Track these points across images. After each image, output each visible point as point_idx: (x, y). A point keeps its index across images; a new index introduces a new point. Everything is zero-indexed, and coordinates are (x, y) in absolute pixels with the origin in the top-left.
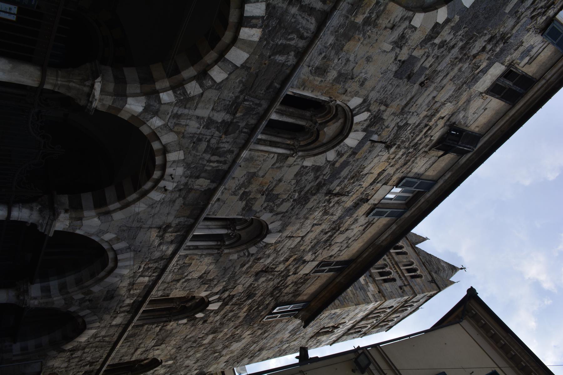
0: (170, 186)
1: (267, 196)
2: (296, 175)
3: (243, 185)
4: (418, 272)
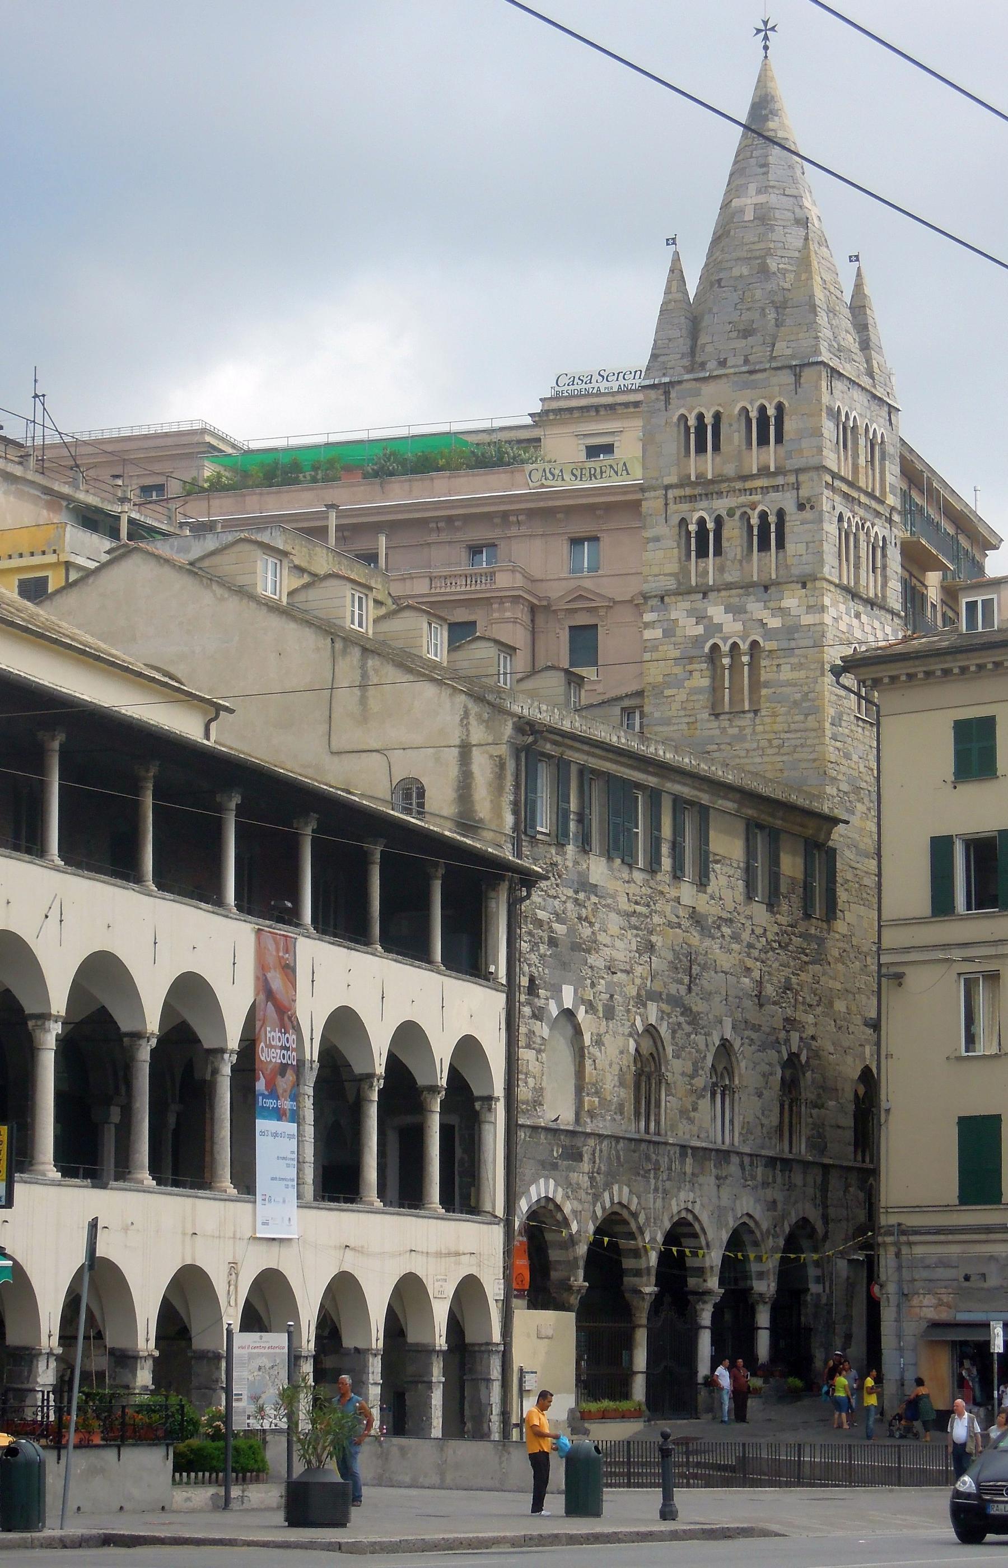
0: (691, 1195)
1: (692, 1077)
3: (689, 1119)
4: (771, 412)
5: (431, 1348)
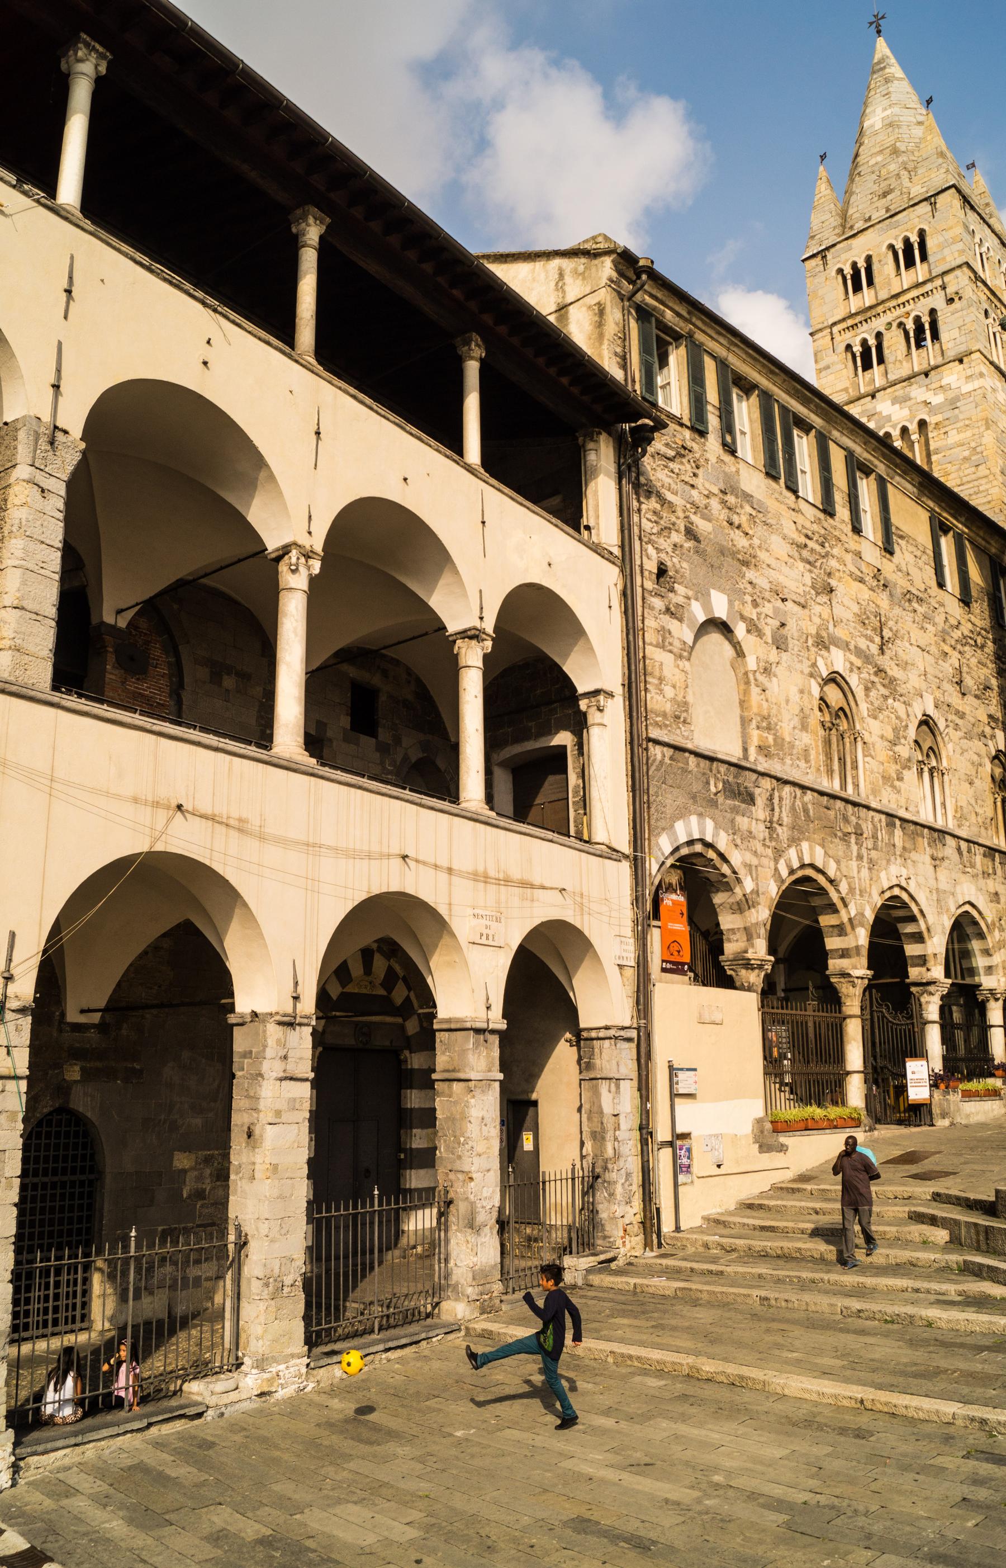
0: (904, 872)
2: (875, 718)
3: (893, 786)
4: (914, 239)
5: (468, 1025)
